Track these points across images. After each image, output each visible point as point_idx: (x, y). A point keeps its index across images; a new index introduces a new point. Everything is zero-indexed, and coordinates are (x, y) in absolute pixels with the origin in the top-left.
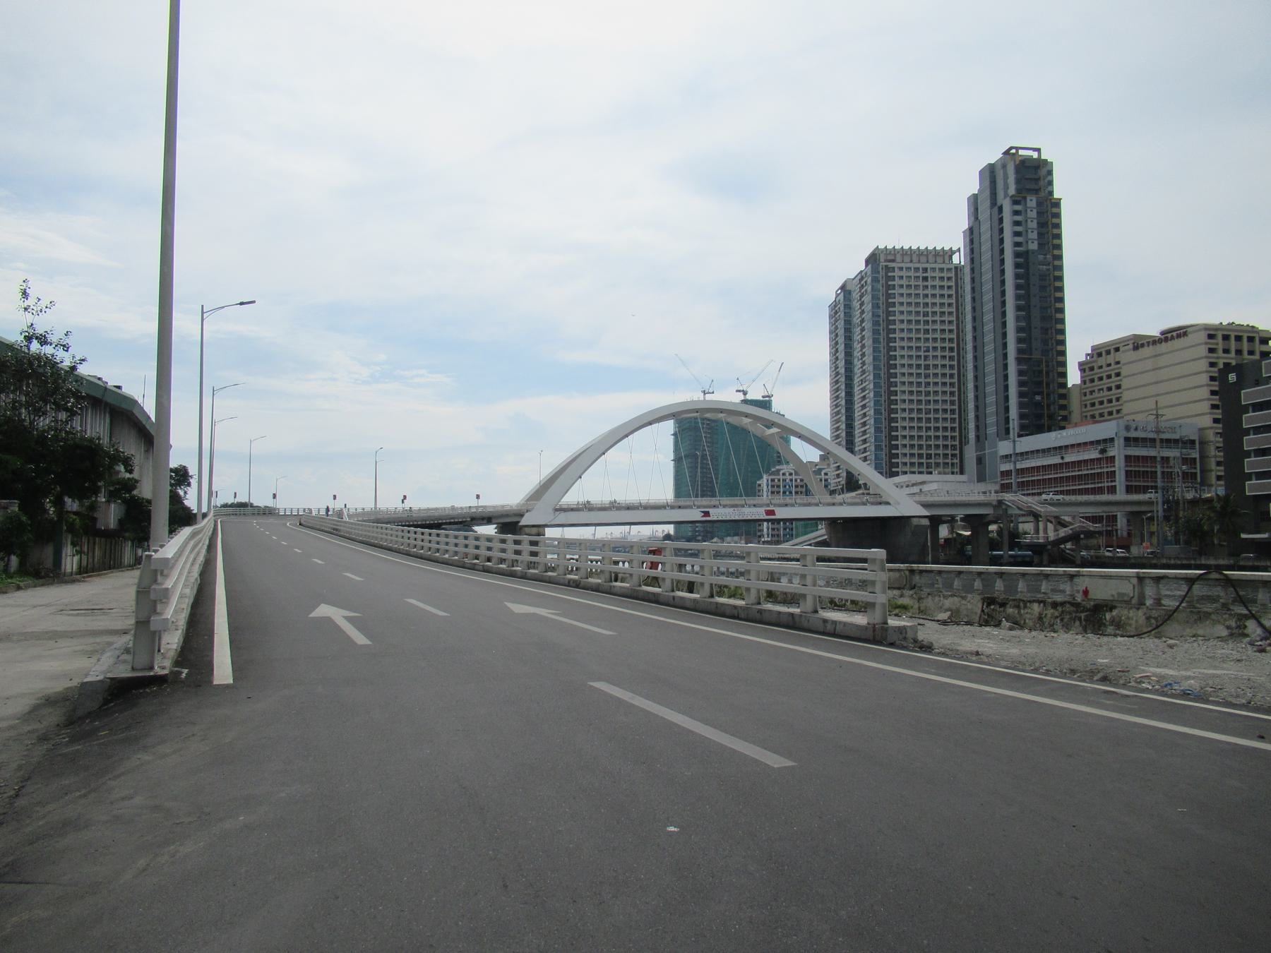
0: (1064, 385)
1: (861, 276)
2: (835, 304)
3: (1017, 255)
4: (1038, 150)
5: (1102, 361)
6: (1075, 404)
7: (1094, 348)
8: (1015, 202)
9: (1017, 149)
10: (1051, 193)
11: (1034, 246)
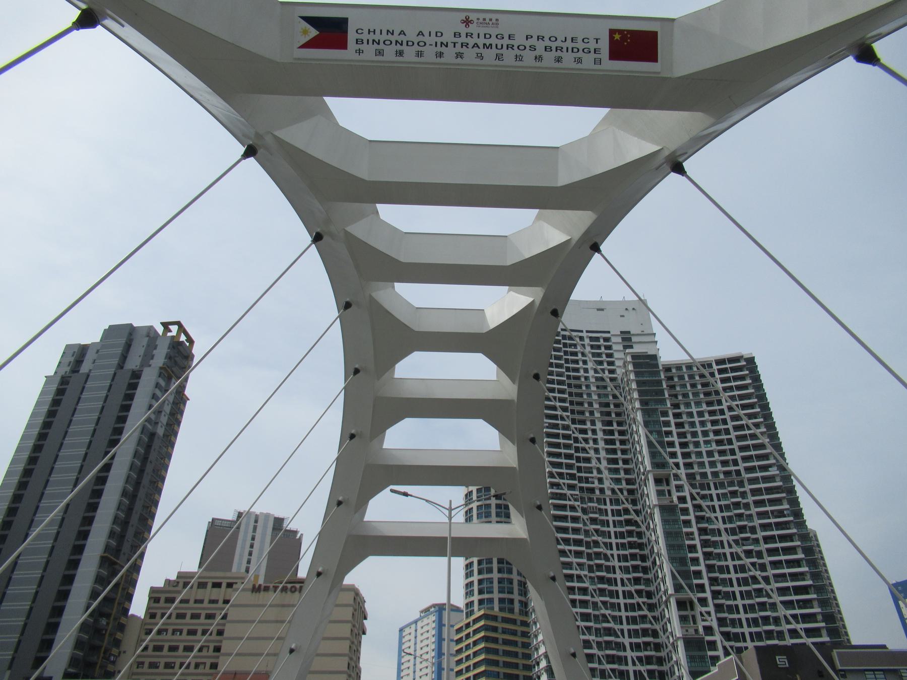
3: (144, 429)
4: (191, 341)
7: (181, 575)
9: (181, 329)
11: (160, 431)
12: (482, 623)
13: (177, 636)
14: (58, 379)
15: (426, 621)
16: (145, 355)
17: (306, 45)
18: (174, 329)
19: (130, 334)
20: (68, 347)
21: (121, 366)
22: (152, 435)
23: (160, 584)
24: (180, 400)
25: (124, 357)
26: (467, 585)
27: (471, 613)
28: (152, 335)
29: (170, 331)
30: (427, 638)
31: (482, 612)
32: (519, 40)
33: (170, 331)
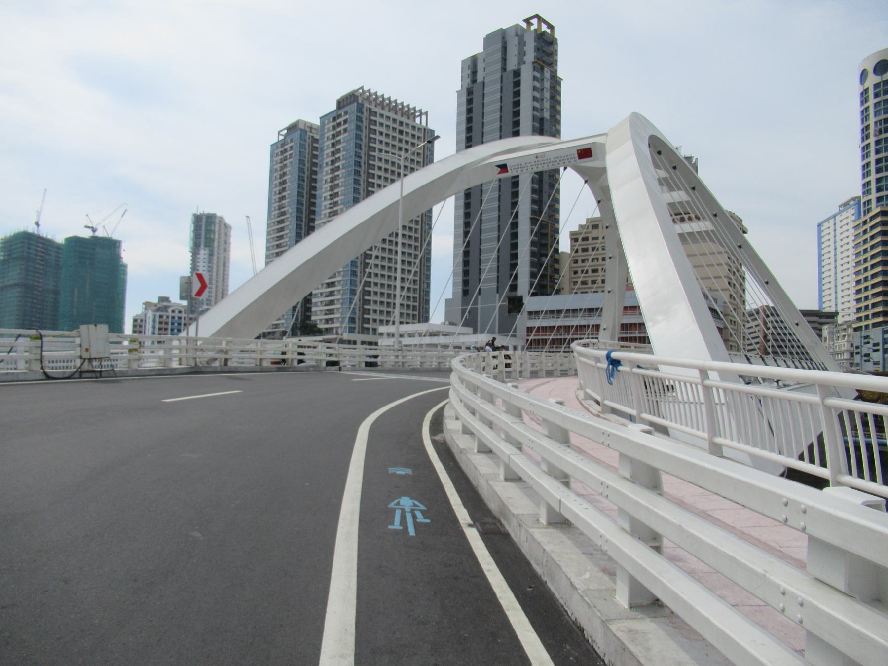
0: (556, 250)
1: (334, 117)
2: (282, 143)
3: (534, 118)
4: (551, 27)
5: (595, 233)
6: (565, 269)
8: (534, 69)
10: (556, 70)
11: (547, 115)
12: (878, 219)
13: (596, 263)
14: (465, 91)
15: (844, 214)
16: (519, 53)
17: (500, 173)
18: (535, 21)
19: (503, 38)
20: (463, 62)
21: (504, 69)
22: (542, 120)
23: (576, 229)
24: (556, 83)
25: (504, 60)
26: (864, 185)
27: (869, 210)
28: (519, 33)
29: (532, 24)
30: (847, 230)
31: (878, 210)
32: (552, 159)
33: (532, 24)
